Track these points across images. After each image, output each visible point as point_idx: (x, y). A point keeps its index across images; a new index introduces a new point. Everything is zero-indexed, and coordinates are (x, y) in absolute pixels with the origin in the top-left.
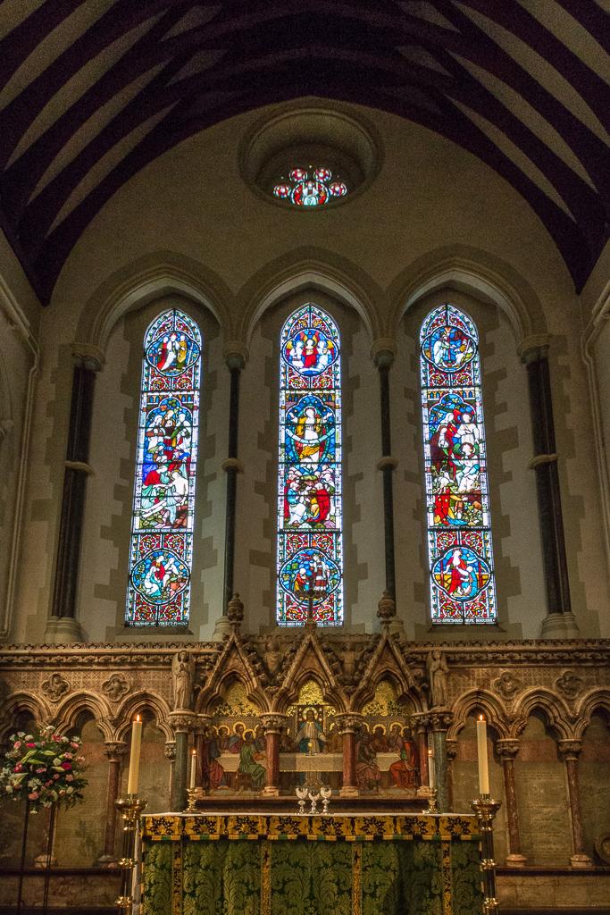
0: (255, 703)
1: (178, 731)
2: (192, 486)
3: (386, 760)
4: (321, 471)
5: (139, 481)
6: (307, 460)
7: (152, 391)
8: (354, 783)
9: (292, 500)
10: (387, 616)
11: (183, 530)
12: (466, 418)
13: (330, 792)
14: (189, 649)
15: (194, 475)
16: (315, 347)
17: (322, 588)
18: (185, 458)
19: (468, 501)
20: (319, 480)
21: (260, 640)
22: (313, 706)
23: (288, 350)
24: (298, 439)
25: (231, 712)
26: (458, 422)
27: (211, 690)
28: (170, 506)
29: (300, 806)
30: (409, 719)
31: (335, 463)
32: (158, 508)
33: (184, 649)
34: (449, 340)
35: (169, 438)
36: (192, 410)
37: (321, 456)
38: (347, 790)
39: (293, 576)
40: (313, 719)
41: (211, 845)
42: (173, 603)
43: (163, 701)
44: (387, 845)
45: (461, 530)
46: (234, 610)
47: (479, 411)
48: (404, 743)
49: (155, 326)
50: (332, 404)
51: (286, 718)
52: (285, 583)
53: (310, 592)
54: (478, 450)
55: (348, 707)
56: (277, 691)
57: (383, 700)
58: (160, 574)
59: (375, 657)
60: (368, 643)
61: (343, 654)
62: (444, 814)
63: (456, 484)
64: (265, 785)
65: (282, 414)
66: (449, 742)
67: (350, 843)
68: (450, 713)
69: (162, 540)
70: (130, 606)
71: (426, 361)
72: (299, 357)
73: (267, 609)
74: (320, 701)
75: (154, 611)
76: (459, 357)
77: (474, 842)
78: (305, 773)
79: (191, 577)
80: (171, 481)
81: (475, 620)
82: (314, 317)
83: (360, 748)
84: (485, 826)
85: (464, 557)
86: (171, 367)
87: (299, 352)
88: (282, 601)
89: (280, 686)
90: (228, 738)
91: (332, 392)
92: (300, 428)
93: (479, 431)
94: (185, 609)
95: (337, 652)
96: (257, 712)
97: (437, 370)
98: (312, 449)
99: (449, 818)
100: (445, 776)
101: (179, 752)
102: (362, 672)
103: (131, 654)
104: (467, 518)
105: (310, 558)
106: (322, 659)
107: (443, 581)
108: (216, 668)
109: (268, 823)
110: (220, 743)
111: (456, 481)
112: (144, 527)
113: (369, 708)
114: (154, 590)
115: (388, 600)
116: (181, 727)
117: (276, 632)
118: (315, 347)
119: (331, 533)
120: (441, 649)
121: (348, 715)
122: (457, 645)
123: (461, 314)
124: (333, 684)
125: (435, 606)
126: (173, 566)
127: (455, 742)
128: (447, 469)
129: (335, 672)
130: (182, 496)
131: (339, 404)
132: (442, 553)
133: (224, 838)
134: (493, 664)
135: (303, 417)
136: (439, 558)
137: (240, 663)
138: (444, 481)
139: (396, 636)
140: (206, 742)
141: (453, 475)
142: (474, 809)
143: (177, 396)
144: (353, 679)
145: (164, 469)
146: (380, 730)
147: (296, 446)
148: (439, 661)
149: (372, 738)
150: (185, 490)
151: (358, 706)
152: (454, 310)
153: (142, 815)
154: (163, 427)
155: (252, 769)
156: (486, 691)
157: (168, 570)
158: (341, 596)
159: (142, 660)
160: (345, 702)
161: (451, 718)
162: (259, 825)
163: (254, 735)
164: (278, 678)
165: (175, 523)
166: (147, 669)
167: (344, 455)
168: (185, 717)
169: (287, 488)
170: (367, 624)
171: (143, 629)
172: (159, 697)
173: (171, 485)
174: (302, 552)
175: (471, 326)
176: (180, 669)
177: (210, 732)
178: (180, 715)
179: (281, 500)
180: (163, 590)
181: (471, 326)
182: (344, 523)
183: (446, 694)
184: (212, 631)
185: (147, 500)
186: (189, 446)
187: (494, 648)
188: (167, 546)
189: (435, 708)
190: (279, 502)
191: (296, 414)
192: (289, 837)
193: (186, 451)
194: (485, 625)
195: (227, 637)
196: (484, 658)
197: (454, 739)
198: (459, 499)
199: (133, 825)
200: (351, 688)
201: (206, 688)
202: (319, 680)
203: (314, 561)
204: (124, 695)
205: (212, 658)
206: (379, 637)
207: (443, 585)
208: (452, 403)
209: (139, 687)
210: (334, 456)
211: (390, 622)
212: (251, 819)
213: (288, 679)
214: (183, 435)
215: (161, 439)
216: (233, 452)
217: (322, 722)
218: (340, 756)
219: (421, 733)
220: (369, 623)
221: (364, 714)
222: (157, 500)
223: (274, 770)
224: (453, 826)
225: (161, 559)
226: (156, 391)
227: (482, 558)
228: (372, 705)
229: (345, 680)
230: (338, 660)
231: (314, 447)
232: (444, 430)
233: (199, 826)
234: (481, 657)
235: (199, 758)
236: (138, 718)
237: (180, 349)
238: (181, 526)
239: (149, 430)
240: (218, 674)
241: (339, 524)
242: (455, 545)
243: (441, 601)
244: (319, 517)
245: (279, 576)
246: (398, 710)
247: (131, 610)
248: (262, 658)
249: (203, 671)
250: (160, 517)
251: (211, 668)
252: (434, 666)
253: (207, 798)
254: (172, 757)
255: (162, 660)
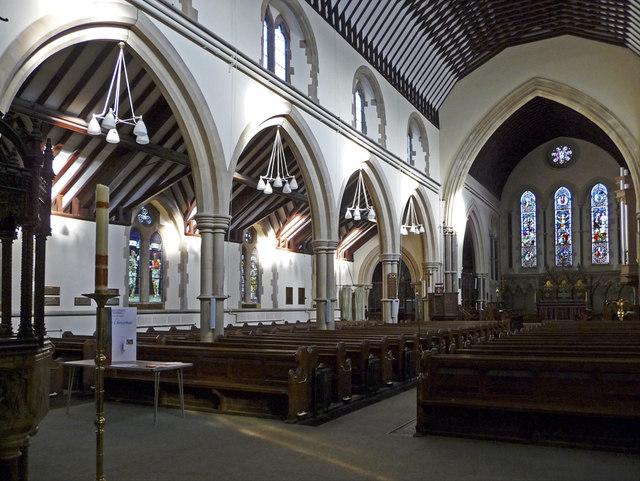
28: (530, 240)
57: (579, 282)
69: (529, 247)
79: (537, 256)
98: (563, 221)
138: (597, 230)
184: (542, 270)
186: (533, 226)
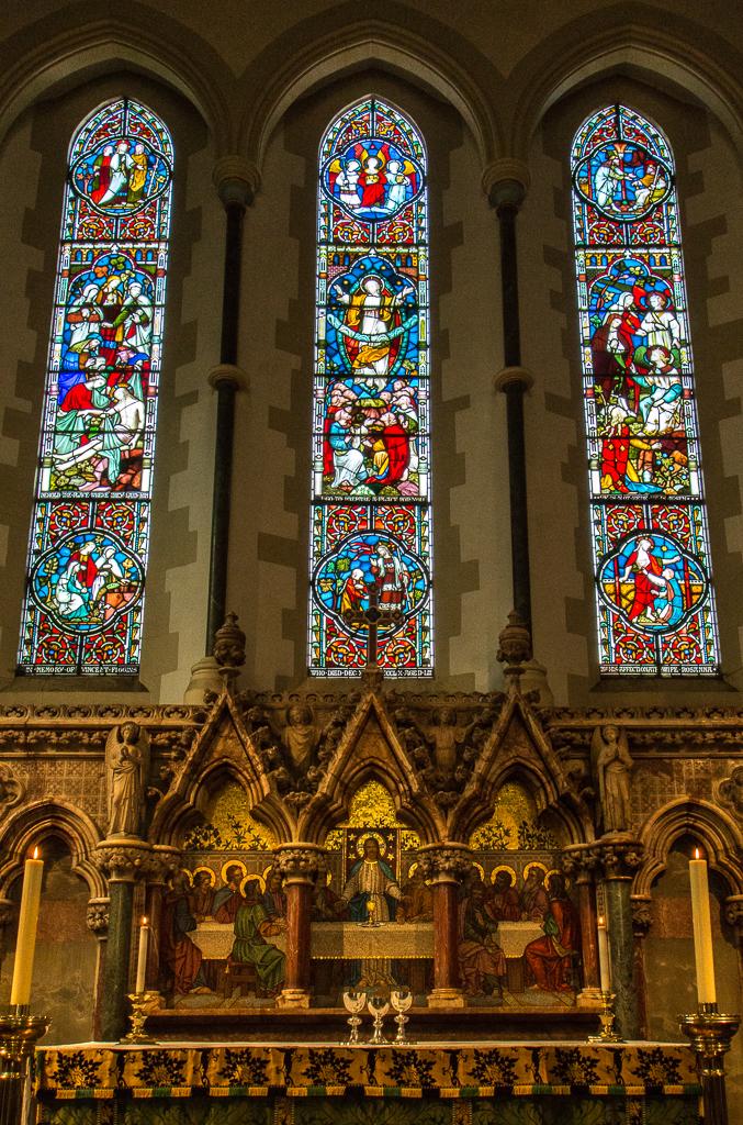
0: (265, 823)
1: (114, 878)
2: (151, 414)
3: (517, 936)
4: (393, 391)
5: (51, 402)
6: (367, 371)
7: (81, 241)
8: (455, 982)
9: (338, 443)
10: (516, 659)
11: (131, 495)
12: (655, 301)
13: (409, 1000)
14: (139, 720)
15: (156, 395)
16: (382, 170)
17: (393, 607)
18: (140, 362)
19: (662, 451)
20: (388, 407)
21: (277, 703)
22: (377, 830)
23: (334, 175)
24: (351, 333)
25: (219, 842)
26: (642, 309)
27: (180, 798)
28: (110, 450)
29: (351, 1027)
30: (559, 855)
31: (418, 377)
32: (86, 452)
33: (130, 720)
34: (623, 164)
35: (109, 325)
36: (154, 277)
37: (391, 364)
38: (442, 996)
39: (340, 583)
40: (377, 856)
41: (174, 1111)
42: (112, 631)
43: (87, 820)
44: (522, 1106)
45: (650, 501)
46: (226, 646)
47: (679, 290)
48: (550, 904)
49: (90, 126)
50: (412, 272)
51: (324, 852)
52: (324, 597)
53: (371, 615)
54: (679, 360)
55: (443, 833)
56: (308, 801)
57: (509, 820)
58: (87, 576)
59: (494, 737)
60: (479, 710)
61: (434, 731)
62: (631, 1044)
63: (640, 419)
64: (283, 985)
65: (321, 287)
66: (635, 901)
67: (449, 1102)
68: (639, 845)
69: (92, 513)
70: (28, 636)
71: (582, 200)
72: (353, 188)
73: (290, 645)
74: (390, 821)
75: (74, 647)
76: (642, 196)
77: (689, 1098)
78: (358, 962)
80: (112, 404)
81: (679, 667)
82: (380, 119)
83: (467, 913)
84: (710, 1068)
85: (657, 553)
86: (117, 200)
87: (353, 179)
88: (318, 630)
89: (313, 790)
90: (213, 893)
91: (413, 250)
92: (353, 314)
93: (679, 326)
94: (135, 642)
95: (423, 729)
96: (269, 842)
97: (602, 217)
99: (639, 1050)
100: (629, 969)
101: (114, 921)
102: (470, 765)
103: (27, 729)
104: (661, 481)
105: (371, 550)
106: (394, 740)
107: (619, 595)
108: (190, 756)
109: (288, 1062)
110: (197, 900)
111: (639, 413)
112: (58, 489)
113: (484, 835)
114: (74, 607)
115: (517, 630)
116: (120, 870)
117: (307, 687)
118: (382, 170)
119: (411, 505)
120: (618, 722)
121: (442, 848)
122: (648, 716)
123: (643, 122)
124: (415, 788)
125: (606, 643)
126: (112, 562)
127: (647, 902)
128: (624, 392)
129: (418, 765)
130: (132, 432)
131: (424, 272)
132: (617, 543)
133: (200, 1093)
134: (716, 752)
135: (359, 294)
136: (610, 554)
137: (240, 747)
138: (619, 412)
139: (533, 698)
140: (169, 901)
141: (634, 403)
142: (688, 1032)
143: (127, 252)
144: (453, 779)
145: (99, 382)
146: (504, 876)
147: (348, 345)
148: (613, 746)
149: (490, 892)
150: (138, 421)
151: (462, 831)
152: (631, 114)
153: (38, 1048)
154: (100, 305)
155: (258, 954)
156: (703, 802)
157: (102, 570)
158: (429, 622)
159: (49, 738)
160: (439, 823)
161: (639, 854)
162: (271, 1066)
163: (263, 886)
164: (310, 775)
165: (118, 481)
166: (59, 758)
167: (435, 364)
168: (130, 851)
169: (330, 420)
170: (478, 675)
171: (52, 681)
172: (79, 812)
173: (111, 411)
174: (358, 539)
175: (661, 142)
176: (121, 756)
177: (178, 881)
178: (118, 846)
179: (318, 443)
180: (92, 606)
181: (661, 142)
182: (436, 485)
183: (627, 807)
184: (183, 684)
185: (66, 439)
186: (147, 340)
187: (716, 721)
188: (102, 526)
189: (608, 836)
190: (315, 447)
191: (346, 289)
192: (330, 1090)
193: (141, 349)
194: (699, 677)
195: (212, 697)
196: (700, 739)
197: (644, 894)
198: (646, 447)
199: (19, 1067)
200: (447, 796)
201: (170, 794)
202: (390, 781)
203: (378, 554)
204: (10, 808)
205: (183, 736)
206: (501, 698)
207: (618, 602)
208: (631, 275)
209: (40, 792)
210: (417, 365)
211: (521, 671)
212: (254, 1055)
213: (328, 778)
214: (137, 320)
215: (95, 328)
216: (229, 353)
217: (394, 861)
218: (427, 927)
219: (584, 884)
220: (479, 670)
221: (474, 846)
222: (85, 440)
223: (300, 956)
224: (648, 1068)
225: (90, 547)
226: (89, 241)
227: (690, 554)
228: (490, 829)
229: (438, 781)
230: (424, 741)
231: (379, 348)
232: (617, 323)
233: (151, 1070)
234: (693, 738)
235: (155, 933)
236: (36, 853)
237: (135, 168)
238: (128, 487)
239: (74, 310)
240: (195, 767)
241: (424, 487)
242: (640, 530)
243: (617, 633)
244: (388, 474)
245: (312, 583)
246: (539, 839)
247: (29, 642)
248: (279, 738)
249: (166, 761)
250: (89, 469)
251: (181, 756)
252: (604, 754)
253: (167, 1012)
254: (102, 930)
255: (86, 741)
